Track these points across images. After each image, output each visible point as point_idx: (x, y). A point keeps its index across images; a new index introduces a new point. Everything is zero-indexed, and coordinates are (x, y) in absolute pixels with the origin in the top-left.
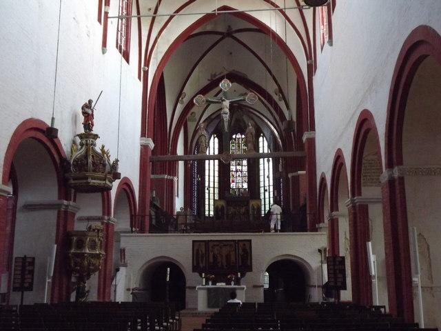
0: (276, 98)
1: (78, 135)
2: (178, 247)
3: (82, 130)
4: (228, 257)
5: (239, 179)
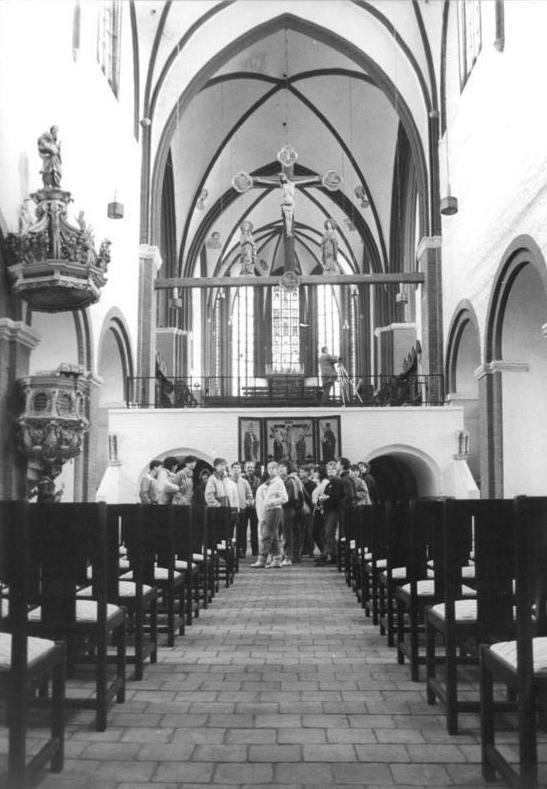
0: (357, 202)
1: (32, 196)
3: (37, 184)
5: (286, 349)
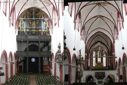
2: (92, 73)
3: (79, 54)
4: (101, 75)
